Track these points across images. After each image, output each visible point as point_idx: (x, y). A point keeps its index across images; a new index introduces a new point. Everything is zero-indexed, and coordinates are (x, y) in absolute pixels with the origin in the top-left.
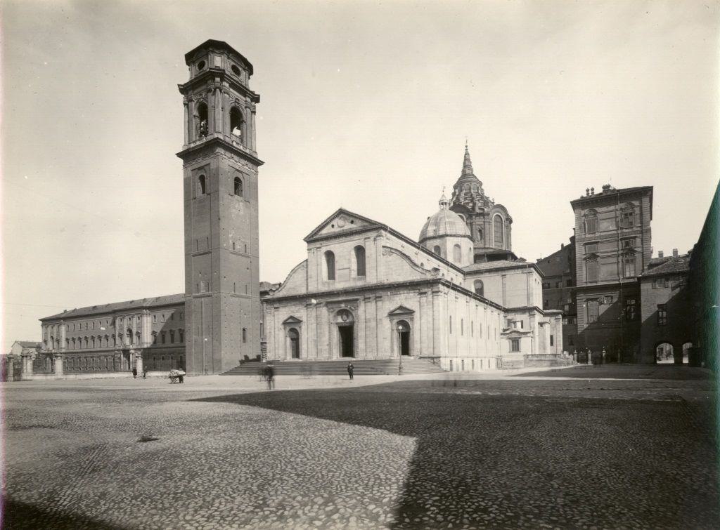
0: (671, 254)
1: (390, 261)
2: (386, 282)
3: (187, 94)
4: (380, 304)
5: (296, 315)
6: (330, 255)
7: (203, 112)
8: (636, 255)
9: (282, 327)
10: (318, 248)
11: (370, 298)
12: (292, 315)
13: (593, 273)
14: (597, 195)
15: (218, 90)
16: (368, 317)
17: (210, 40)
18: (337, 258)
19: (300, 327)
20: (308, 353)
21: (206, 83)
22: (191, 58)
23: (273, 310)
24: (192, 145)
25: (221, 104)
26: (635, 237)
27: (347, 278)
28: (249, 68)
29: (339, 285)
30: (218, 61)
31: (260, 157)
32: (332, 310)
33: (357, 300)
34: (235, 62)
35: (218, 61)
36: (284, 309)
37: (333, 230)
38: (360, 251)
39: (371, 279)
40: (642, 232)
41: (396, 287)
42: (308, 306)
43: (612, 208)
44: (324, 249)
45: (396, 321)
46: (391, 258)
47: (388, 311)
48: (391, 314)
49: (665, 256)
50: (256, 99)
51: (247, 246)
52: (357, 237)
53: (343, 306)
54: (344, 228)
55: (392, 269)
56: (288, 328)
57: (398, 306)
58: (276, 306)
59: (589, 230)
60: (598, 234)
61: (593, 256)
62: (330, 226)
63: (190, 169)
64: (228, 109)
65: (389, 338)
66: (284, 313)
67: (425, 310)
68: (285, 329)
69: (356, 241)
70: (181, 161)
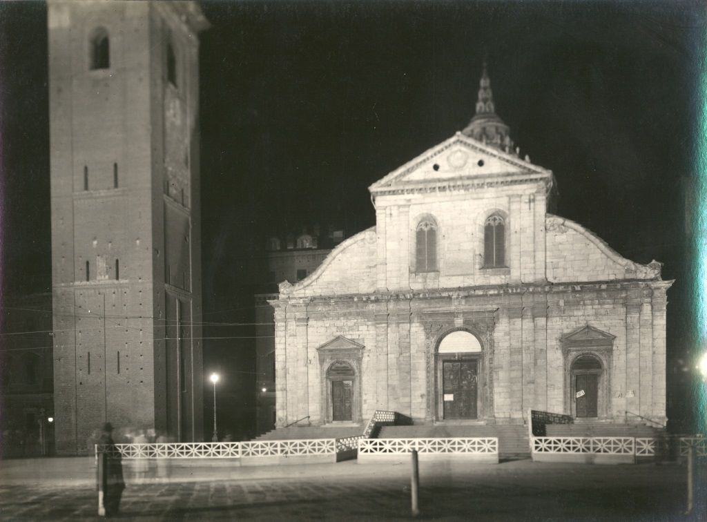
1: (560, 244)
4: (541, 321)
10: (399, 206)
12: (338, 334)
16: (516, 344)
19: (359, 360)
23: (292, 325)
36: (320, 323)
44: (416, 212)
45: (573, 355)
46: (561, 238)
47: (558, 335)
55: (565, 257)
56: (326, 366)
57: (583, 324)
65: (561, 385)
66: (320, 332)
67: (634, 336)
68: (322, 361)
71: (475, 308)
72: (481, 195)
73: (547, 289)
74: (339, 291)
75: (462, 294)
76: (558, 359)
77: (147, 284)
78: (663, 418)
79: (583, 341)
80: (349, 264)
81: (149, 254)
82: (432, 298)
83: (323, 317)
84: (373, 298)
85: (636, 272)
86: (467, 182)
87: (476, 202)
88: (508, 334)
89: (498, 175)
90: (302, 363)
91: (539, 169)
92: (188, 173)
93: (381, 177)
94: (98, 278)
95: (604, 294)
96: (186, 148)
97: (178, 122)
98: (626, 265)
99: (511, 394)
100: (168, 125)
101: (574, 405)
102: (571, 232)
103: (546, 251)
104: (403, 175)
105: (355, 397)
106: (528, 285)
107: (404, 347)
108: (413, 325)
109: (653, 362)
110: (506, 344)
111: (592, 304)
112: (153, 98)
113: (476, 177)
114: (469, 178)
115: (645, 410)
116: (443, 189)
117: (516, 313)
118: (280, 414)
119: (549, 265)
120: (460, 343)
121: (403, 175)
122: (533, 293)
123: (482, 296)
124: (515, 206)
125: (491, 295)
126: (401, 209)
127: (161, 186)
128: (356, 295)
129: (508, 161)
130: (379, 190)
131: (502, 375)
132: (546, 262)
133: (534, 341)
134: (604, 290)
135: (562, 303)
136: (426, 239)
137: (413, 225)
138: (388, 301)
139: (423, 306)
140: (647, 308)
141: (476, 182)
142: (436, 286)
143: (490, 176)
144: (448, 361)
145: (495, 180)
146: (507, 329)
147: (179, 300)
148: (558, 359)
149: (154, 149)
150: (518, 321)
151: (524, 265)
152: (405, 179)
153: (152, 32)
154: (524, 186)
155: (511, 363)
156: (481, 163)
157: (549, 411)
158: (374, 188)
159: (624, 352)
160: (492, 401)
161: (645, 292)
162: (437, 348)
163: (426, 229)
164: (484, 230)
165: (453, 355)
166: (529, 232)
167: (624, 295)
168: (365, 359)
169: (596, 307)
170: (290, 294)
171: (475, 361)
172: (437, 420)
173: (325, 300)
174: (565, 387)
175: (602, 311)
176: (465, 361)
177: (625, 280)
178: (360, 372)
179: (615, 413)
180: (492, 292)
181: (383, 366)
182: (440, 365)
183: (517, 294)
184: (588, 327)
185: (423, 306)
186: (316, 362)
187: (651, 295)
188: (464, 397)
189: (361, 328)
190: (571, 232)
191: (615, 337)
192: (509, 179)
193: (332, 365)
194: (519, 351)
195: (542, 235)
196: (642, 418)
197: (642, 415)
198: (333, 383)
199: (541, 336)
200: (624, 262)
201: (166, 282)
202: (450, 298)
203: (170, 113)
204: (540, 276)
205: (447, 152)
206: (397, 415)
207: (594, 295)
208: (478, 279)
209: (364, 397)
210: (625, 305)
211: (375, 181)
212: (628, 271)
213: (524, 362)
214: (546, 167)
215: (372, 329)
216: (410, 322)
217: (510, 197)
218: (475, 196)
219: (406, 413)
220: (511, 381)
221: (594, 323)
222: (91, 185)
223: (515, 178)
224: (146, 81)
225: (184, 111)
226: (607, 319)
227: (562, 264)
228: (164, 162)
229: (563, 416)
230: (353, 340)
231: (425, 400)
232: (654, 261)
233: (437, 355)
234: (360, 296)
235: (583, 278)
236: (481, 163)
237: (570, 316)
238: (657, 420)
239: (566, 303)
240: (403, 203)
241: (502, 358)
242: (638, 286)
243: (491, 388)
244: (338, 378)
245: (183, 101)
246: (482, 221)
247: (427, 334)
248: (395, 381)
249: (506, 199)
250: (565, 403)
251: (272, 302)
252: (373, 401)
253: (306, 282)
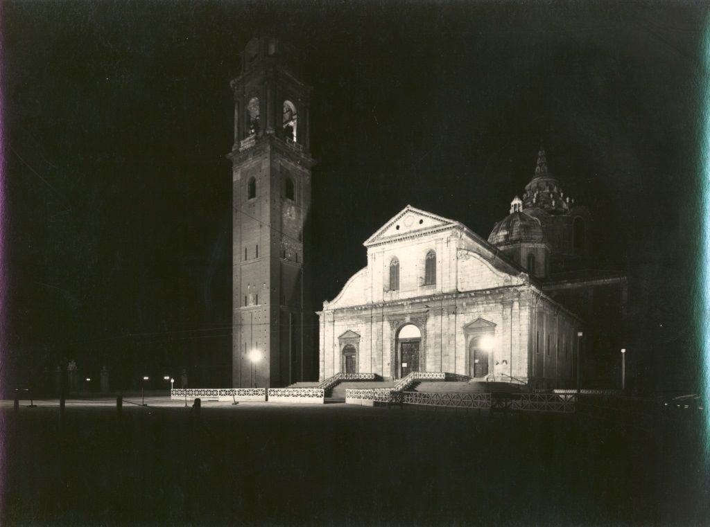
4: (452, 317)
5: (354, 329)
9: (337, 341)
29: (403, 294)
46: (466, 263)
47: (462, 325)
51: (299, 253)
52: (425, 239)
55: (468, 275)
56: (343, 347)
57: (476, 317)
62: (394, 226)
65: (464, 356)
68: (340, 345)
71: (416, 311)
72: (421, 241)
73: (454, 296)
74: (351, 304)
75: (409, 302)
76: (462, 340)
77: (268, 307)
78: (525, 378)
79: (477, 328)
80: (361, 288)
81: (268, 291)
82: (394, 306)
83: (342, 319)
84: (363, 307)
85: (511, 281)
86: (412, 235)
87: (418, 246)
88: (434, 325)
89: (430, 228)
90: (331, 346)
91: (451, 221)
92: (301, 245)
93: (368, 238)
94: (250, 304)
95: (490, 297)
96: (300, 233)
97: (294, 218)
98: (505, 277)
99: (435, 362)
100: (285, 221)
101: (472, 370)
102: (472, 258)
103: (457, 272)
104: (381, 233)
105: (357, 366)
106: (447, 294)
107: (381, 334)
108: (385, 322)
109: (520, 341)
110: (433, 332)
111: (483, 304)
112: (272, 209)
113: (419, 231)
114: (414, 232)
115: (515, 373)
117: (440, 312)
118: (321, 374)
119: (459, 280)
120: (410, 332)
121: (381, 233)
122: (447, 299)
123: (419, 303)
124: (439, 246)
125: (425, 302)
126: (380, 255)
127: (277, 255)
128: (356, 307)
129: (435, 218)
130: (370, 244)
131: (430, 351)
132: (457, 279)
133: (448, 329)
134: (488, 295)
135: (464, 304)
136: (394, 270)
137: (388, 264)
138: (372, 309)
139: (389, 310)
140: (516, 305)
141: (417, 233)
142: (397, 299)
143: (425, 229)
144: (405, 343)
145: (427, 231)
146: (434, 323)
147: (292, 314)
148: (462, 340)
149: (272, 236)
150: (439, 317)
151: (444, 283)
152: (382, 237)
153: (272, 174)
154: (443, 233)
155: (436, 343)
156: (421, 222)
157: (457, 373)
158: (365, 244)
159: (501, 334)
160: (425, 367)
161: (515, 294)
162: (397, 335)
163: (395, 265)
164: (425, 262)
165: (406, 339)
166: (447, 261)
167: (502, 297)
168: (361, 343)
169: (485, 305)
170: (328, 306)
171: (418, 342)
172: (397, 378)
173: (342, 310)
174: (466, 358)
175: (488, 308)
176: (413, 343)
177: (504, 287)
178: (358, 350)
179: (496, 375)
180: (424, 300)
181: (369, 347)
182: (399, 346)
183: (439, 300)
184: (479, 319)
185: (389, 310)
186: (338, 345)
187: (519, 296)
188: (412, 365)
189: (359, 325)
190: (472, 258)
191: (496, 325)
192: (435, 229)
193: (346, 346)
194: (441, 336)
195: (454, 263)
196: (512, 378)
197: (513, 376)
198: (347, 357)
199: (452, 326)
200: (504, 275)
201: (281, 304)
202: (402, 305)
203: (287, 215)
204: (453, 288)
205: (403, 218)
206: (375, 374)
207: (483, 298)
208: (420, 292)
209: (360, 365)
210: (502, 303)
211: (366, 240)
212: (506, 281)
213: (443, 343)
214: (455, 219)
215: (364, 325)
216: (383, 321)
217: (436, 240)
218: (417, 242)
219: (380, 374)
220: (435, 355)
221: (484, 317)
222: (248, 257)
223: (438, 228)
224: (269, 202)
225: (298, 212)
226: (492, 313)
227: (466, 279)
228: (281, 240)
229: (465, 376)
230: (355, 333)
231: (390, 367)
232: (522, 273)
233: (397, 340)
234: (357, 307)
235: (480, 288)
236: (421, 222)
237: (469, 313)
238: (521, 380)
239: (467, 304)
240: (381, 250)
241: (431, 341)
242: (509, 291)
243: (425, 359)
244: (349, 354)
245: (298, 206)
246: (423, 257)
247: (391, 327)
248: (375, 356)
249: (434, 242)
250: (466, 368)
251: (318, 313)
252: (365, 367)
253: (335, 300)
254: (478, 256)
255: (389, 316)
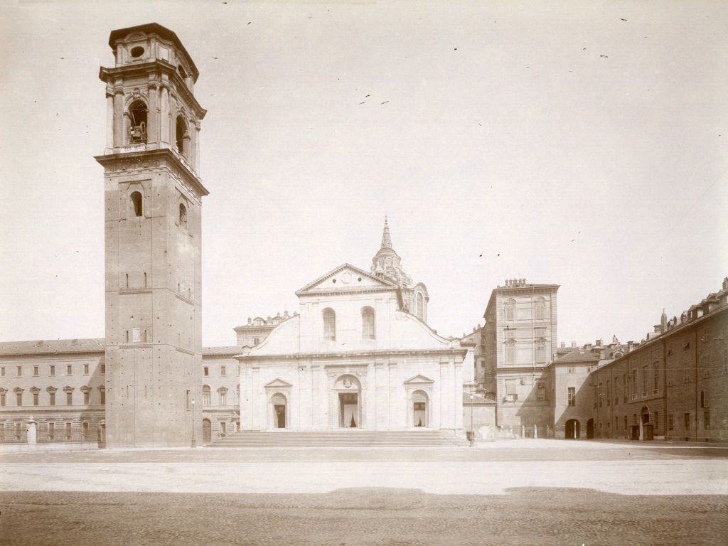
0: (570, 346)
2: (401, 349)
3: (113, 82)
4: (393, 371)
6: (329, 314)
7: (139, 114)
8: (546, 343)
9: (262, 390)
11: (382, 364)
13: (511, 355)
14: (527, 285)
15: (165, 91)
17: (155, 24)
18: (337, 319)
20: (296, 420)
21: (148, 76)
22: (117, 38)
23: (250, 371)
24: (123, 151)
25: (163, 107)
26: (546, 328)
27: (350, 337)
28: (195, 74)
30: (165, 53)
31: (205, 184)
32: (333, 375)
33: (366, 365)
34: (182, 63)
35: (165, 53)
37: (335, 285)
38: (368, 313)
39: (381, 345)
40: (551, 324)
41: (415, 355)
42: (301, 368)
43: (529, 299)
44: (323, 306)
47: (403, 380)
48: (407, 383)
49: (567, 346)
50: (201, 114)
53: (347, 371)
54: (349, 285)
57: (417, 375)
58: (254, 366)
59: (508, 317)
60: (516, 322)
61: (512, 341)
63: (116, 181)
64: (175, 117)
68: (267, 393)
69: (368, 300)
70: (102, 168)
116: (337, 294)
152: (317, 287)
156: (360, 280)
236: (360, 280)
240: (316, 301)
254: (417, 320)
255: (327, 367)
